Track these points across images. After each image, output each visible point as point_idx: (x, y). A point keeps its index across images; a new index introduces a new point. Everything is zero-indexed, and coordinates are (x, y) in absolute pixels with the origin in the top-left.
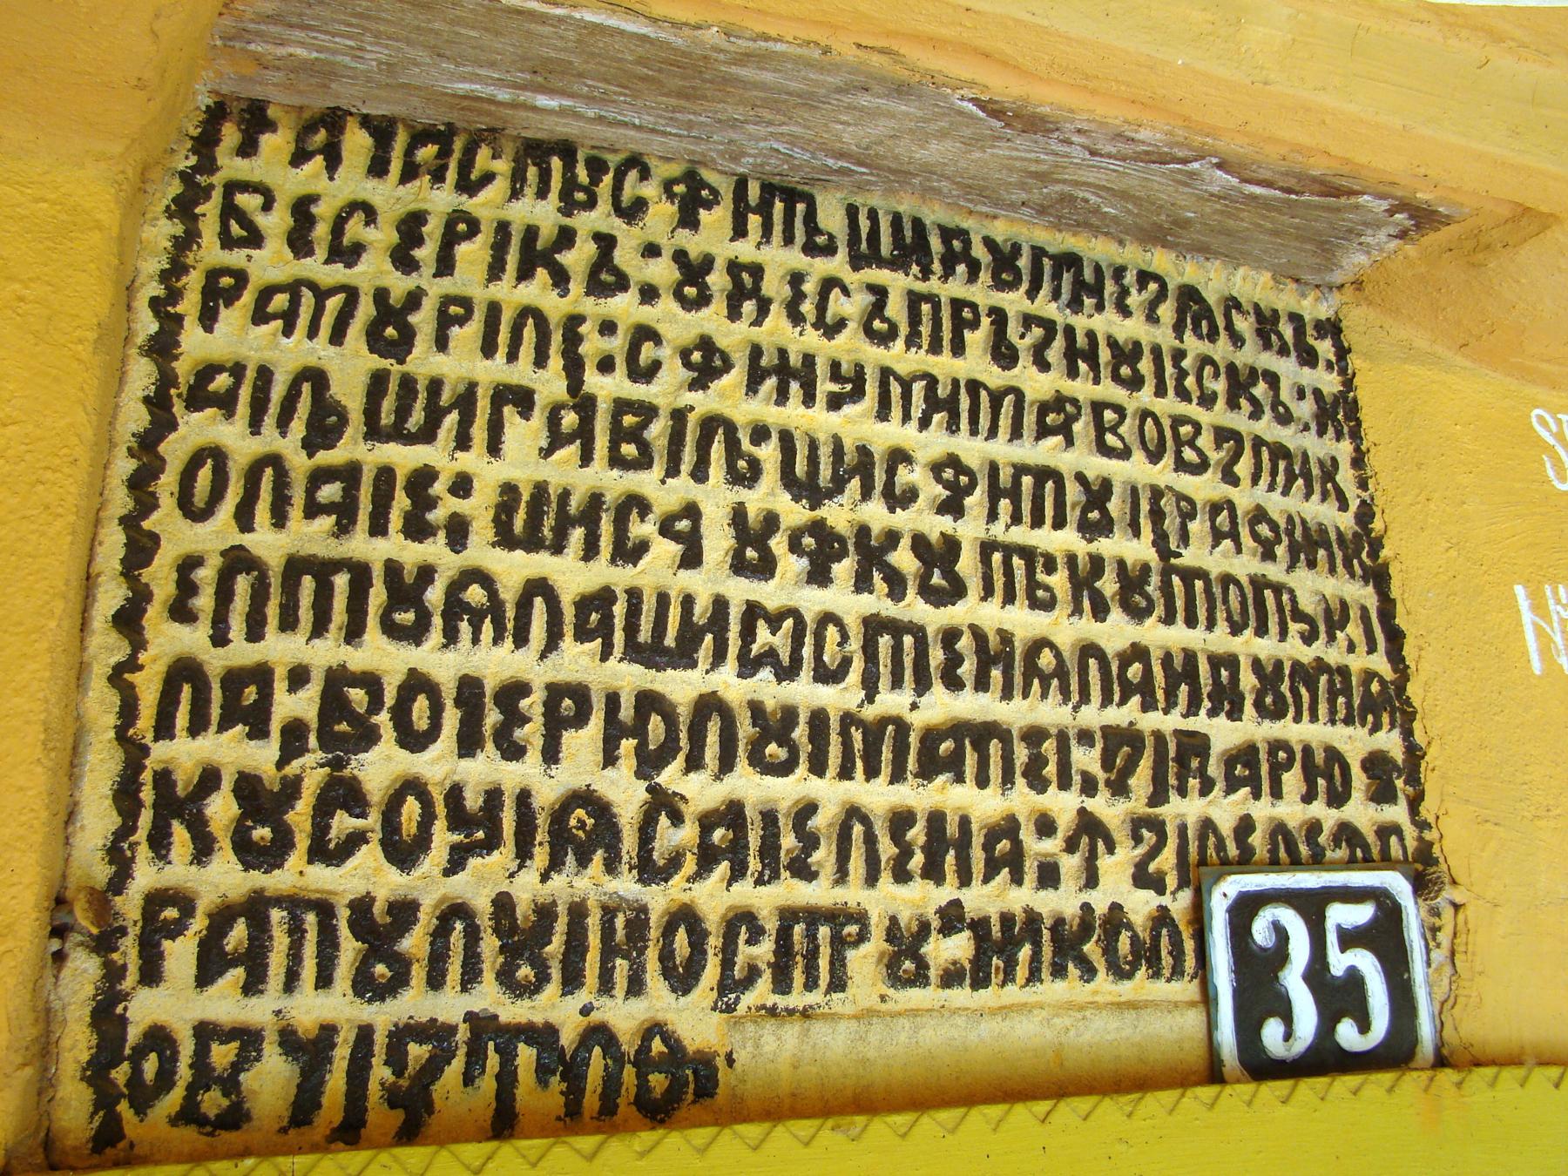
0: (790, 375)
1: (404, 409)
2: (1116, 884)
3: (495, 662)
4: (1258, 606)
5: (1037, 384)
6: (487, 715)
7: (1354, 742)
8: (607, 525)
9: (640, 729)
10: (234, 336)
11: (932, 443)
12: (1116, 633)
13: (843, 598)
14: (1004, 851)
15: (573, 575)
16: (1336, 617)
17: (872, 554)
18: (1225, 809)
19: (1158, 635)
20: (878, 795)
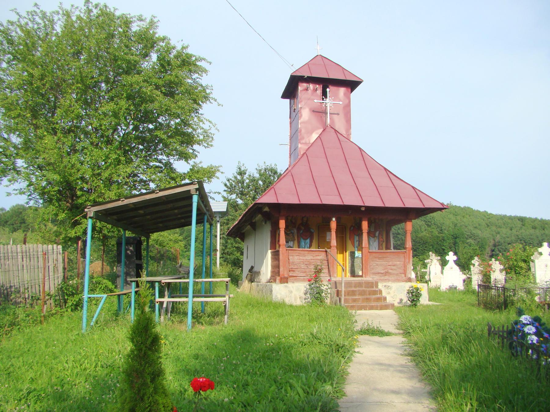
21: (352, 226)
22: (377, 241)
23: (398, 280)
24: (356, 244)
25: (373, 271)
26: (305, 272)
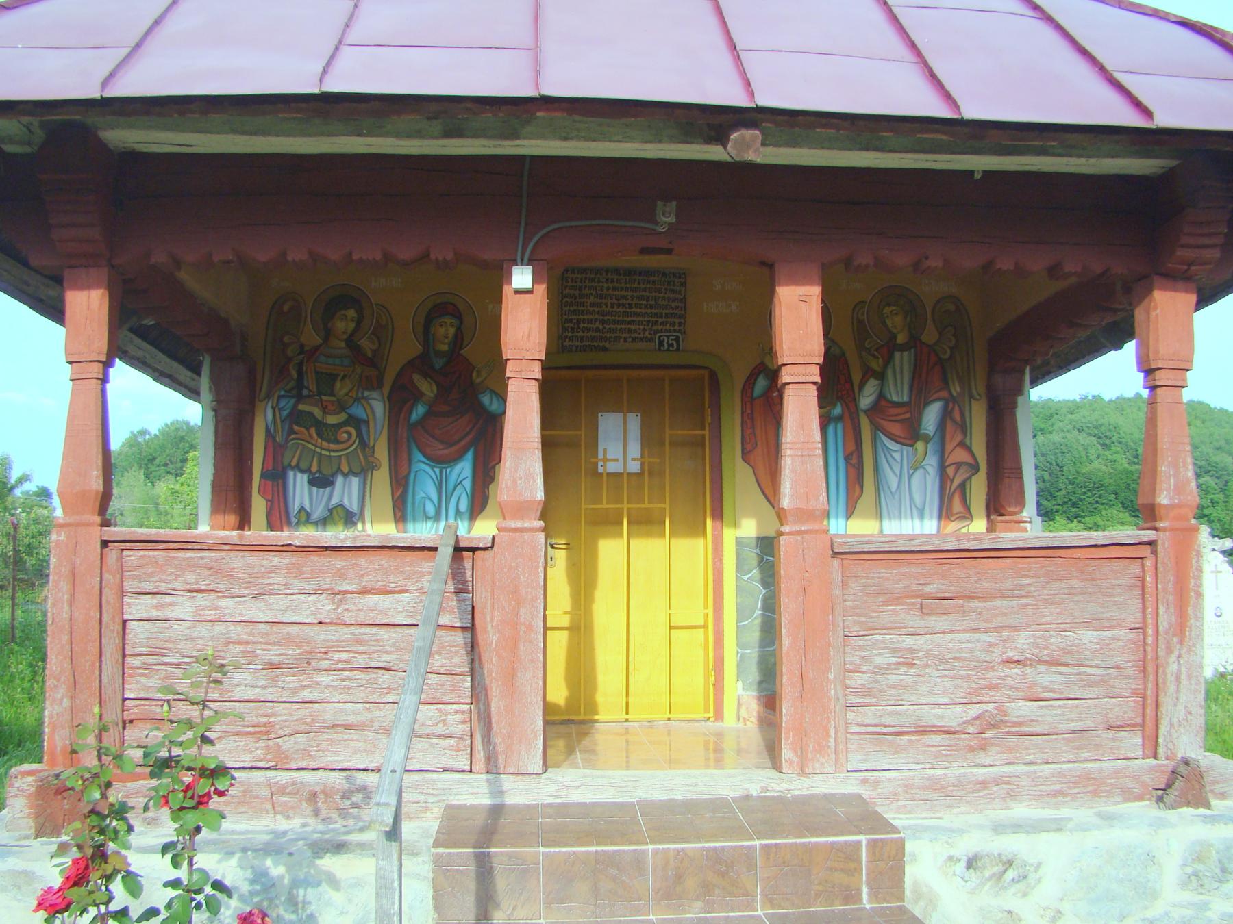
0: (615, 289)
1: (581, 296)
3: (591, 317)
6: (590, 321)
7: (677, 321)
8: (600, 305)
9: (603, 322)
10: (567, 291)
12: (649, 311)
13: (621, 309)
14: (635, 331)
15: (596, 309)
16: (677, 308)
17: (623, 305)
22: (932, 462)
23: (1090, 787)
25: (870, 715)
26: (266, 730)
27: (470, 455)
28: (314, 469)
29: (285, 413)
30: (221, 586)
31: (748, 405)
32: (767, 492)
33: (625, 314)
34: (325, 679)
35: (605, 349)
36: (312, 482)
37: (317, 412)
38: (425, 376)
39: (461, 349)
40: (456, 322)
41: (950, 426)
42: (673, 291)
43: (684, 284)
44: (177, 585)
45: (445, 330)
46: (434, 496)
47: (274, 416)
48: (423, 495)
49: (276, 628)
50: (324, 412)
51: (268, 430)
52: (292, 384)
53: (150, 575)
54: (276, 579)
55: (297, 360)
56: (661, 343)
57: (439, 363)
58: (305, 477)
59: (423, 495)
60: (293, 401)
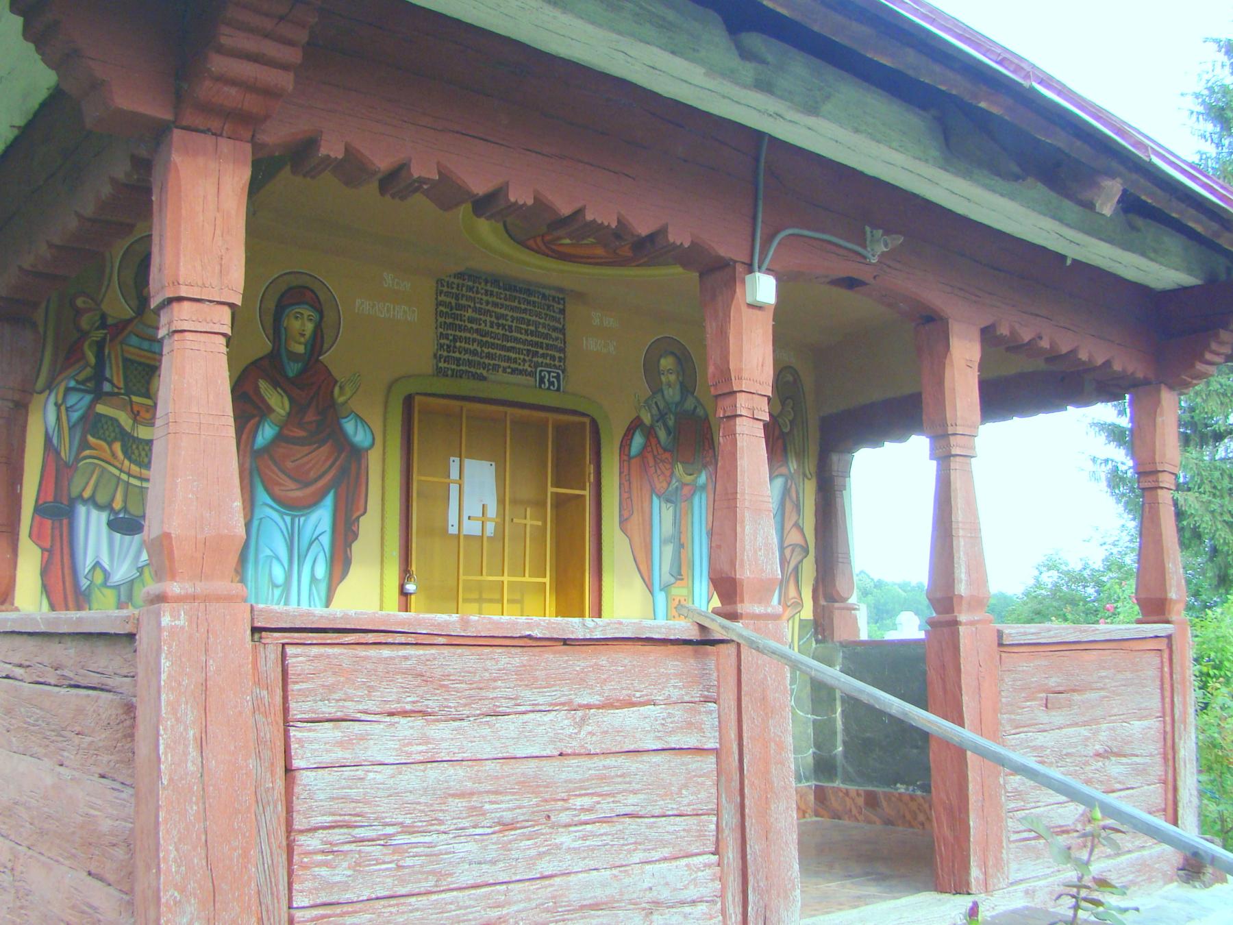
0: (495, 305)
1: (459, 307)
2: (526, 367)
3: (468, 335)
4: (546, 336)
5: (523, 306)
6: (467, 340)
7: (557, 355)
11: (510, 314)
12: (529, 338)
13: (501, 331)
14: (515, 361)
15: (475, 326)
16: (557, 339)
17: (504, 326)
18: (540, 360)
19: (534, 339)
20: (503, 353)
21: (635, 425)
24: (663, 558)
27: (329, 501)
28: (118, 505)
29: (75, 416)
30: (432, 705)
31: (626, 464)
32: (641, 568)
33: (507, 339)
34: (565, 839)
35: (483, 378)
36: (113, 525)
37: (124, 419)
38: (275, 384)
39: (320, 355)
40: (316, 316)
41: (789, 506)
42: (553, 319)
43: (562, 311)
44: (370, 705)
45: (301, 324)
46: (283, 553)
47: (58, 419)
48: (268, 552)
49: (508, 768)
50: (135, 420)
51: (48, 439)
52: (88, 372)
53: (331, 689)
54: (503, 689)
55: (98, 335)
56: (542, 380)
57: (293, 369)
58: (104, 516)
59: (268, 552)
60: (88, 398)
